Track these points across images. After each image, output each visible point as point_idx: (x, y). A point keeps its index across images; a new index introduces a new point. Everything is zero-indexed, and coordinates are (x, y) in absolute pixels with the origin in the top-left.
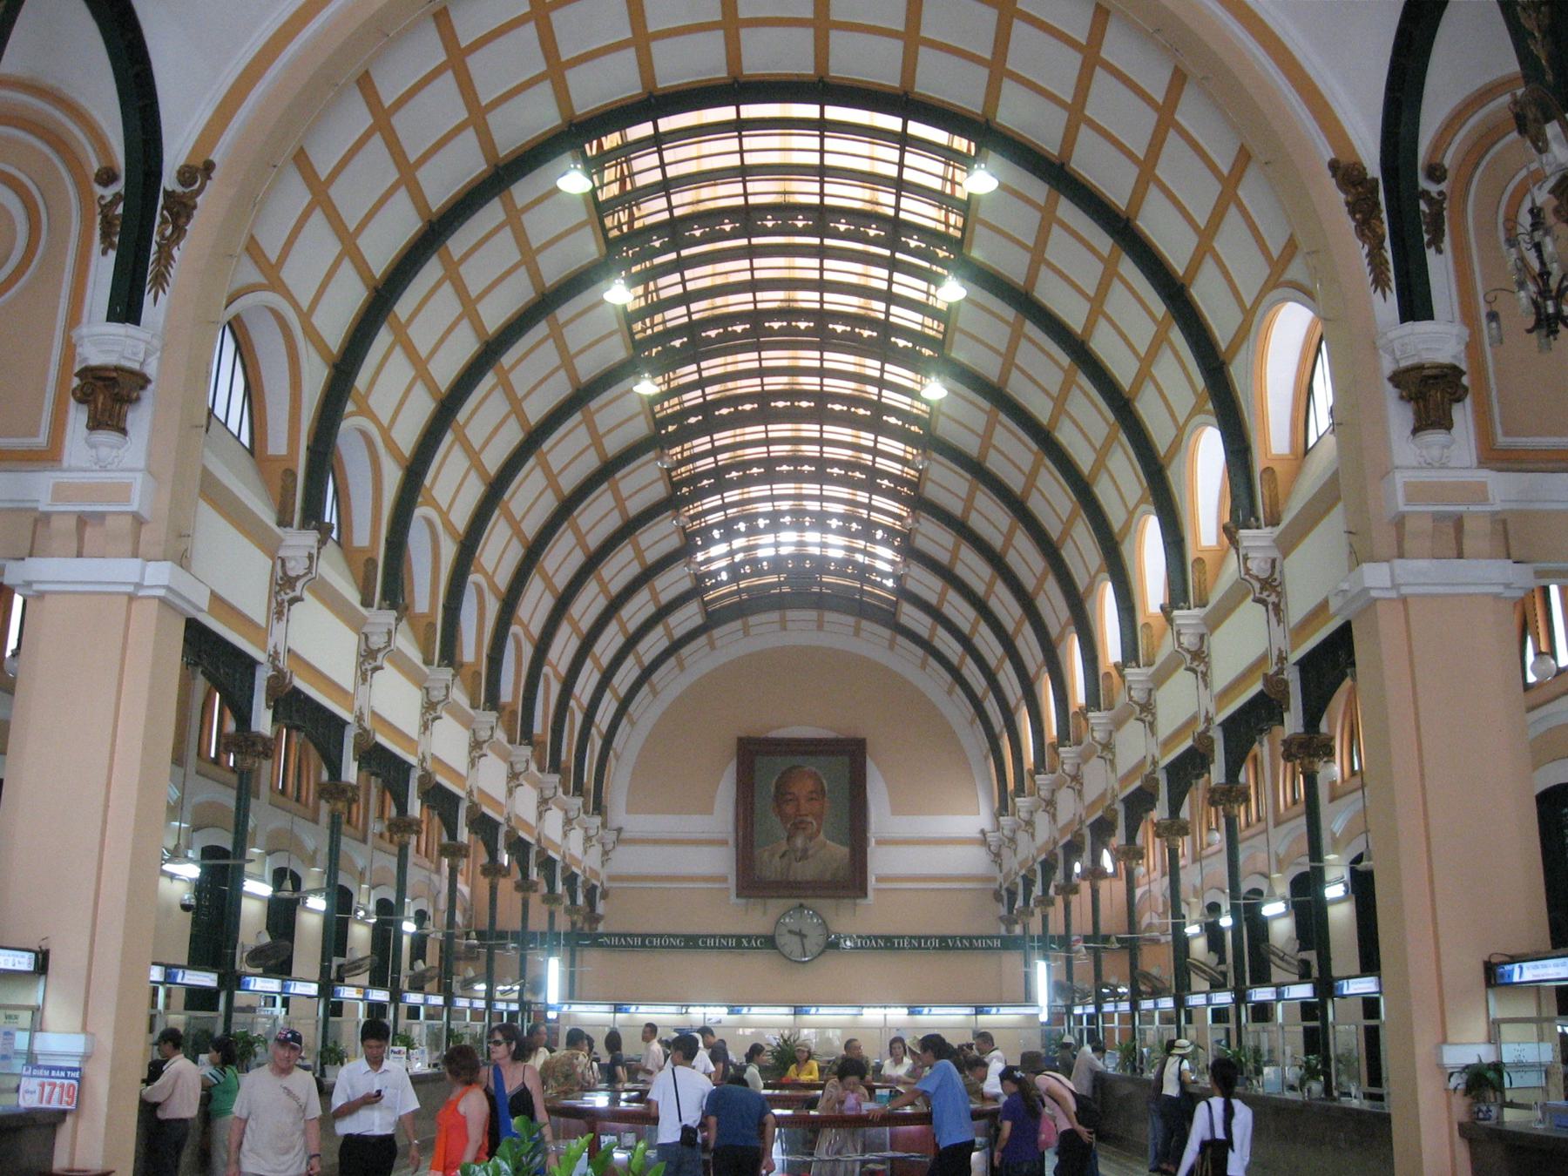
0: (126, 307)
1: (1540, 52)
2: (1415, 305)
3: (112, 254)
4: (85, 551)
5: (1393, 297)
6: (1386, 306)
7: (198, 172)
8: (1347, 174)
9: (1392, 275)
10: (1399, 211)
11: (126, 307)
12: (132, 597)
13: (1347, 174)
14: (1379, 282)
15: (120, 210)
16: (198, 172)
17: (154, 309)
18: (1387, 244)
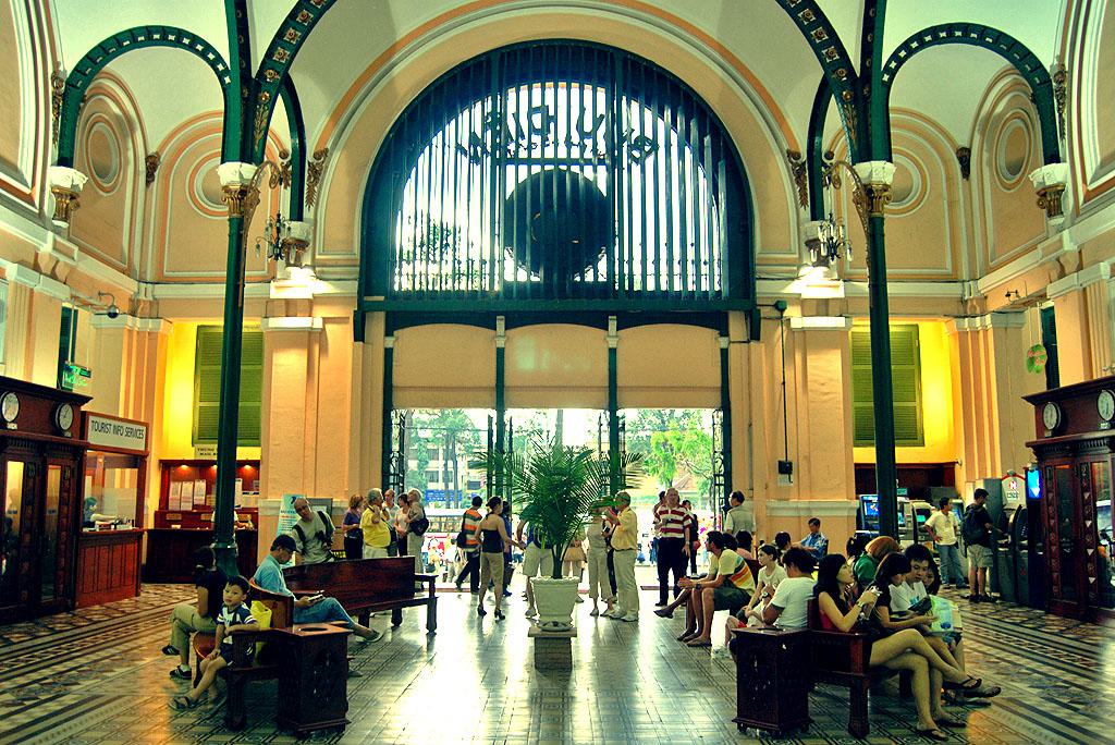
0: (297, 215)
1: (853, 137)
2: (817, 214)
3: (289, 188)
4: (290, 313)
5: (809, 209)
6: (806, 213)
7: (322, 154)
8: (792, 155)
9: (809, 199)
10: (812, 173)
11: (297, 215)
12: (310, 333)
13: (792, 155)
14: (804, 203)
15: (290, 169)
16: (322, 154)
17: (308, 213)
18: (808, 187)
